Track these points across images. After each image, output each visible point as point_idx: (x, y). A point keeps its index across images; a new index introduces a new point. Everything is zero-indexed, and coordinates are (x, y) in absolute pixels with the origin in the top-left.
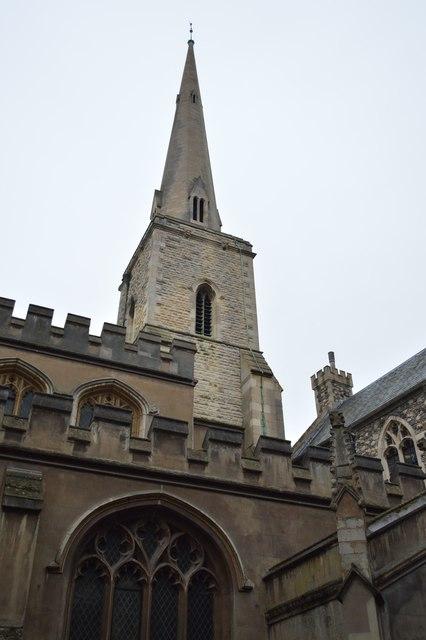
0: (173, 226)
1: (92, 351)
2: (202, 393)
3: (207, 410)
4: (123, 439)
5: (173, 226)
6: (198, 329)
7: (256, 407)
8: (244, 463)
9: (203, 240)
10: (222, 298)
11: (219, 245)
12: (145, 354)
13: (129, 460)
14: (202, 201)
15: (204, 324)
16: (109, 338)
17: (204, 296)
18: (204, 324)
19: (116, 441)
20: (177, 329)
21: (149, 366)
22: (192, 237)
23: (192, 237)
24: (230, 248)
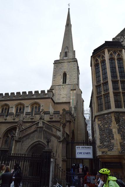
0: (57, 62)
1: (32, 97)
2: (62, 97)
3: (63, 100)
4: (12, 117)
5: (57, 62)
6: (63, 83)
7: (72, 97)
8: (31, 118)
9: (64, 62)
10: (68, 74)
11: (68, 62)
12: (42, 95)
13: (12, 121)
14: (67, 52)
15: (65, 81)
16: (35, 94)
17: (65, 75)
18: (65, 81)
19: (11, 118)
20: (57, 85)
21: (42, 97)
22: (62, 63)
23: (62, 63)
24: (70, 62)
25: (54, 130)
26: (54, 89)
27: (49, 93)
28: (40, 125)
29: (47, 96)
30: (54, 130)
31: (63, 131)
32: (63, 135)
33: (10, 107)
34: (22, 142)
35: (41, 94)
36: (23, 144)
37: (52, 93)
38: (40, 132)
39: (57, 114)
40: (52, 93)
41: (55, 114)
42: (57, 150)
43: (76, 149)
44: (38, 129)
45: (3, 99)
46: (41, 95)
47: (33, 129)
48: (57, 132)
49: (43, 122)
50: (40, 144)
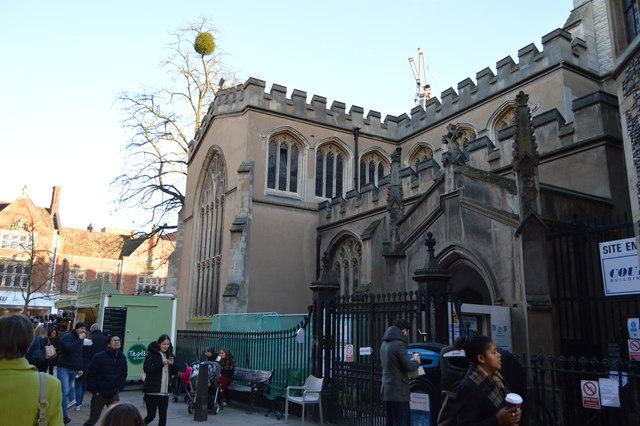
1: (494, 89)
25: (495, 191)
26: (580, 21)
27: (552, 45)
28: (449, 187)
29: (545, 64)
30: (495, 196)
31: (525, 189)
32: (526, 205)
33: (434, 149)
34: (410, 259)
35: (521, 63)
36: (412, 263)
37: (569, 40)
38: (454, 211)
39: (549, 122)
40: (569, 40)
41: (542, 128)
42: (513, 270)
43: (602, 255)
44: (448, 203)
45: (410, 131)
46: (522, 68)
47: (432, 203)
48: (504, 201)
49: (455, 173)
50: (458, 257)
